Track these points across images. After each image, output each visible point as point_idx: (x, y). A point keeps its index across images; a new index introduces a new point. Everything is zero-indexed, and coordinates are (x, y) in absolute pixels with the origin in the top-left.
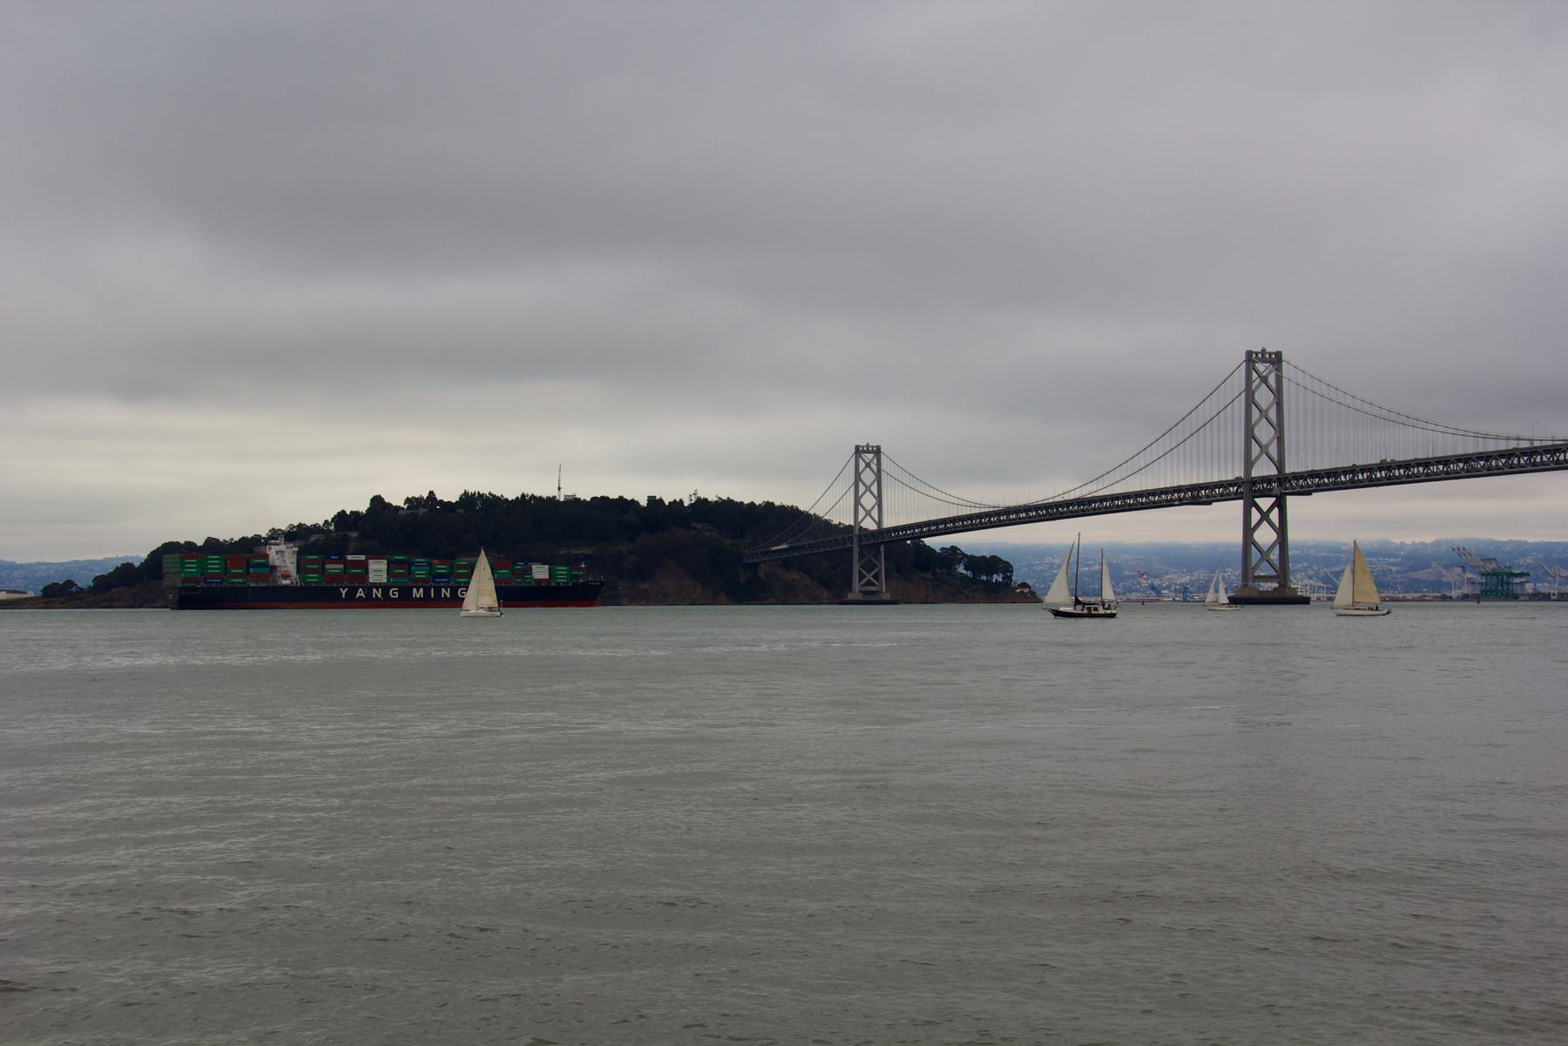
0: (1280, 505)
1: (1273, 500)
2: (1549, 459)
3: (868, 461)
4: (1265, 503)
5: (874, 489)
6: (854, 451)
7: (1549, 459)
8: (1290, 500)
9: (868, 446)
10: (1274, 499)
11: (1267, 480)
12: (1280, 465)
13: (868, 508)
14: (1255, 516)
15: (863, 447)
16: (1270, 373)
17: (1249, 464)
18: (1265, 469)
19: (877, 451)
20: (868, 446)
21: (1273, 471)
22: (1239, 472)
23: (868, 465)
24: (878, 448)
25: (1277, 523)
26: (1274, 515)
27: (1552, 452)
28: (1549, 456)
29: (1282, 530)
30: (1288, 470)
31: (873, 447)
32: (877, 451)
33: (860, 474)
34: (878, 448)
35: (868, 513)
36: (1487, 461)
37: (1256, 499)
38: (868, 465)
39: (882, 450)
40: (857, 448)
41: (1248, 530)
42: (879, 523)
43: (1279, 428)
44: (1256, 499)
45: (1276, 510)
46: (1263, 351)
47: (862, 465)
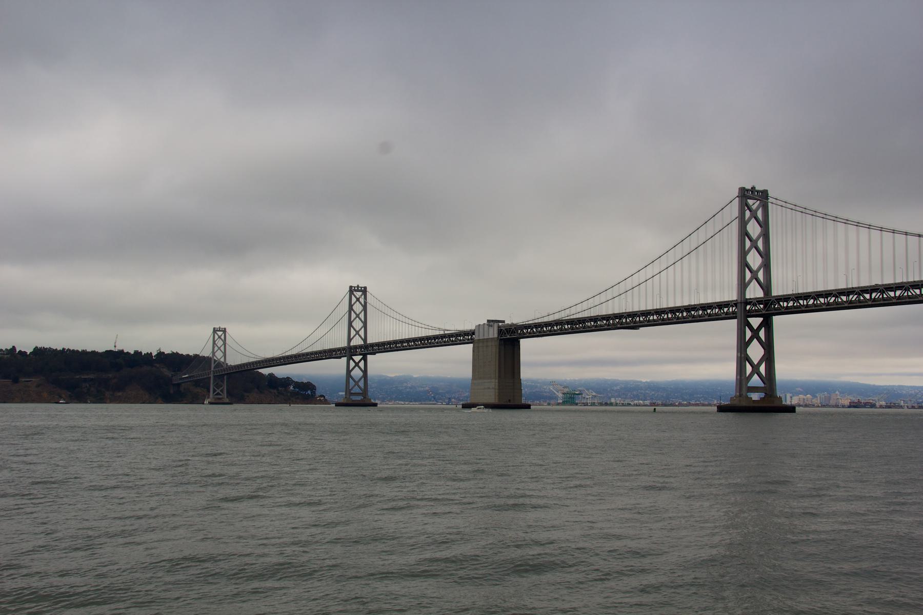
0: (767, 324)
1: (761, 319)
2: (658, 317)
3: (358, 297)
4: (755, 322)
5: (362, 316)
6: (348, 289)
7: (658, 317)
8: (777, 320)
9: (358, 286)
10: (761, 319)
11: (759, 301)
12: (766, 287)
13: (357, 329)
14: (749, 334)
15: (355, 287)
16: (758, 209)
17: (743, 285)
18: (754, 292)
19: (364, 291)
20: (358, 286)
21: (760, 294)
22: (732, 295)
23: (358, 300)
24: (365, 288)
25: (763, 338)
26: (762, 334)
28: (644, 317)
29: (768, 347)
30: (776, 292)
31: (361, 288)
32: (364, 291)
33: (352, 306)
34: (365, 288)
35: (357, 333)
37: (749, 319)
38: (358, 300)
39: (367, 290)
40: (351, 287)
41: (743, 345)
42: (365, 340)
43: (766, 256)
44: (750, 320)
45: (763, 330)
46: (753, 188)
47: (354, 299)
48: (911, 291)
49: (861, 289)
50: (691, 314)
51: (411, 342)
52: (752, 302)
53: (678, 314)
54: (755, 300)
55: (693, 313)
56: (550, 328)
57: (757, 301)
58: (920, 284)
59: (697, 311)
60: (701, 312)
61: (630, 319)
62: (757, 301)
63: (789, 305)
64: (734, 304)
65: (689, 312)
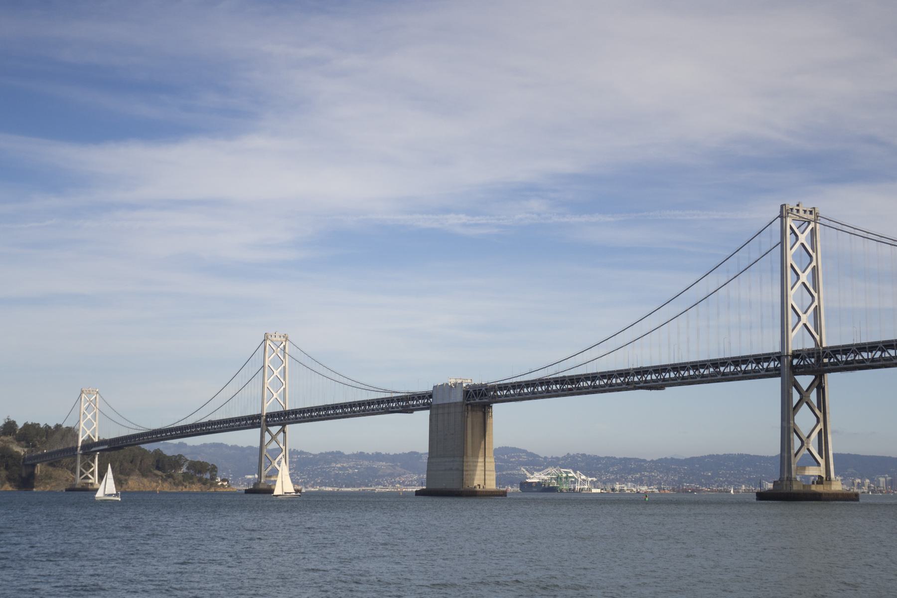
27: (642, 374)
36: (609, 379)
48: (807, 359)
49: (712, 362)
50: (700, 372)
51: (347, 408)
52: (800, 354)
53: (682, 372)
54: (731, 360)
55: (702, 371)
56: (518, 390)
57: (831, 351)
58: (740, 360)
59: (727, 367)
60: (712, 370)
61: (639, 377)
62: (831, 351)
63: (849, 359)
64: (777, 357)
65: (697, 369)
